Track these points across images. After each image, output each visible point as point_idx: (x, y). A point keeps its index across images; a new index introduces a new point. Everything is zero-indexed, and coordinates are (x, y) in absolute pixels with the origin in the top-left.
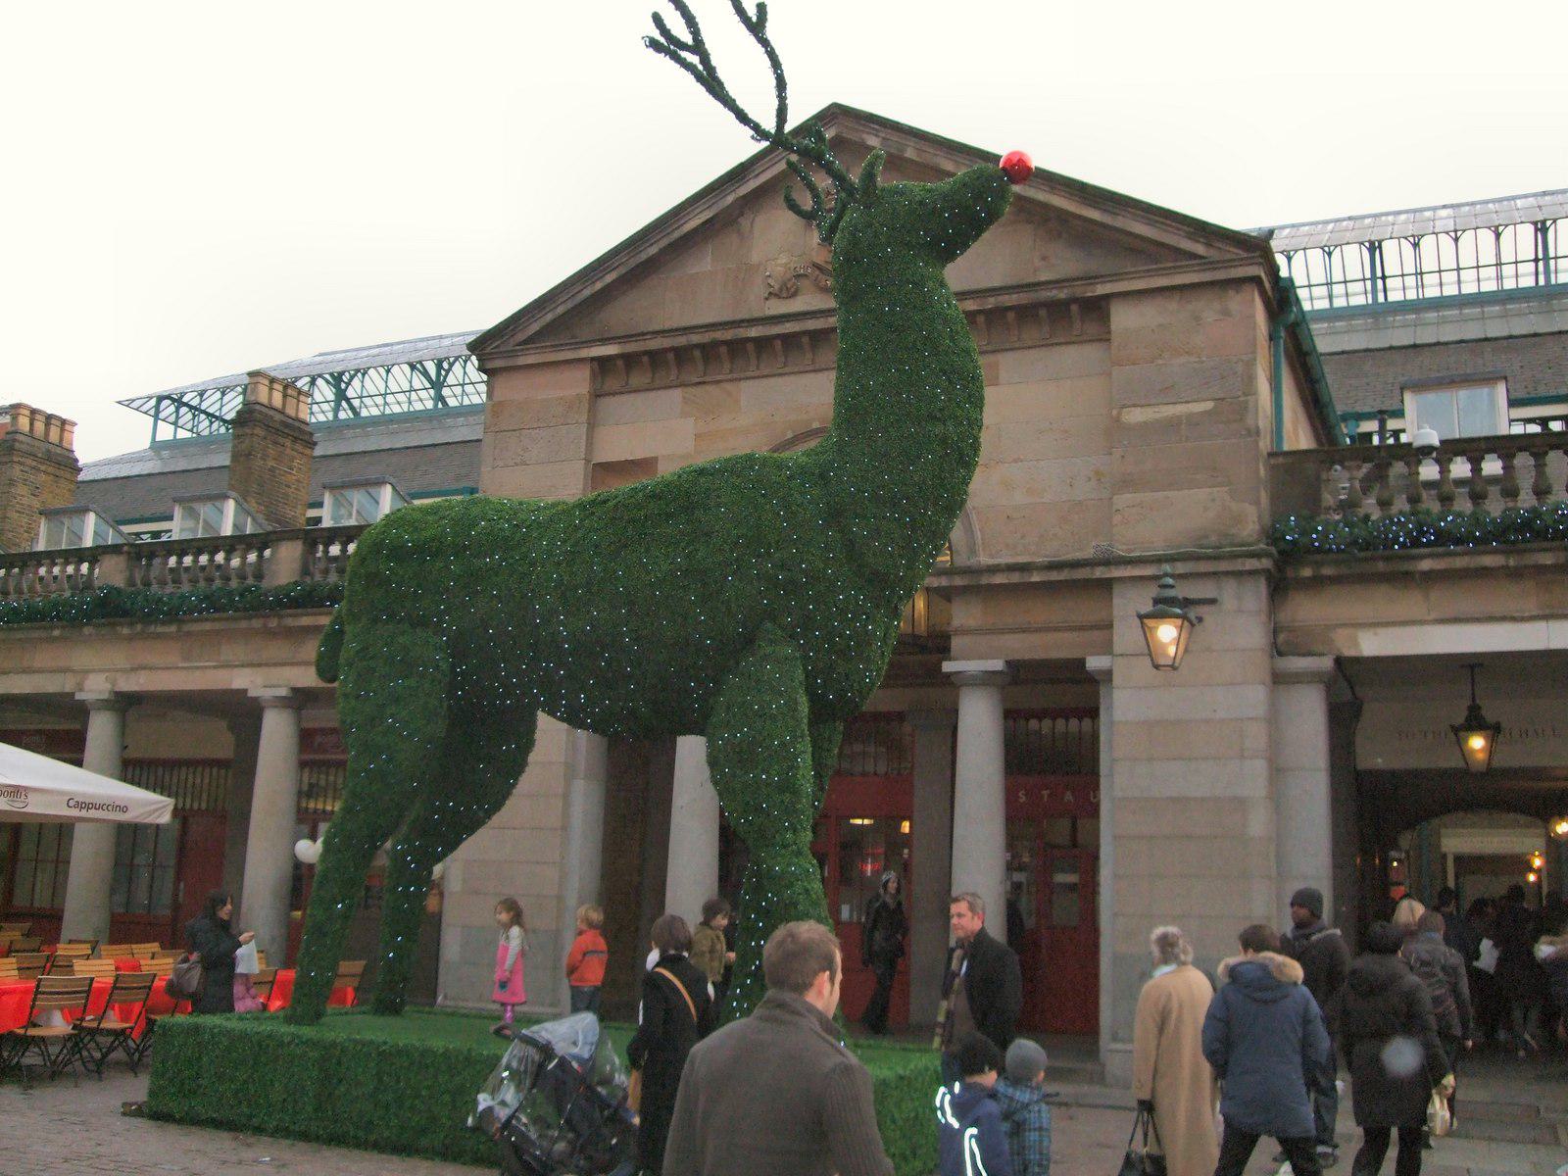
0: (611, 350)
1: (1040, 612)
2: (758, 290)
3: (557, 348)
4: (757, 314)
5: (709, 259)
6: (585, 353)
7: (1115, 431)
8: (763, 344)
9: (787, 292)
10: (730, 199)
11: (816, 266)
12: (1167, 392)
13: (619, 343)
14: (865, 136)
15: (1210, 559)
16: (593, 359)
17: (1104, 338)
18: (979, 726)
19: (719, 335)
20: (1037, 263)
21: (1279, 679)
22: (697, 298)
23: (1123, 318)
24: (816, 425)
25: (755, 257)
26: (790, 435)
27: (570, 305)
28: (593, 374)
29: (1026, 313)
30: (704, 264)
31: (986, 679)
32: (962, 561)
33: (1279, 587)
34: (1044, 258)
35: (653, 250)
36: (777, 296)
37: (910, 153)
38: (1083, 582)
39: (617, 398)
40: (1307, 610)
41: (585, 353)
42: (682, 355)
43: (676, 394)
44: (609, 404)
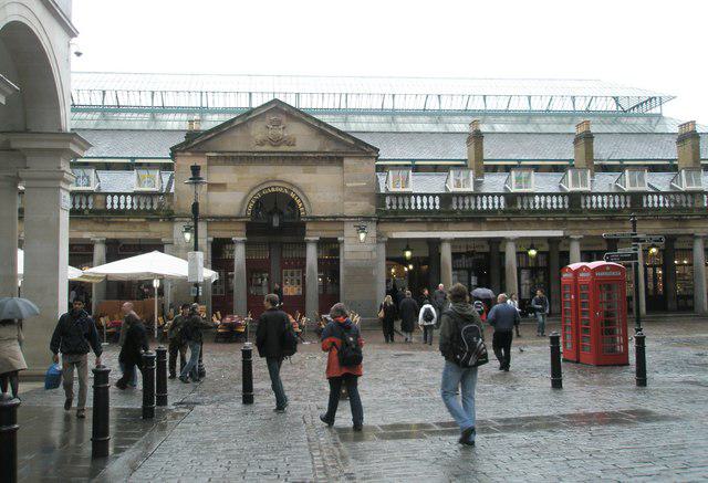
0: (214, 154)
1: (327, 227)
7: (344, 187)
9: (262, 144)
12: (357, 180)
15: (366, 218)
17: (341, 164)
18: (312, 254)
21: (378, 242)
22: (236, 143)
23: (347, 162)
25: (252, 133)
30: (238, 133)
31: (315, 242)
33: (378, 223)
38: (338, 220)
40: (384, 228)
44: (211, 167)
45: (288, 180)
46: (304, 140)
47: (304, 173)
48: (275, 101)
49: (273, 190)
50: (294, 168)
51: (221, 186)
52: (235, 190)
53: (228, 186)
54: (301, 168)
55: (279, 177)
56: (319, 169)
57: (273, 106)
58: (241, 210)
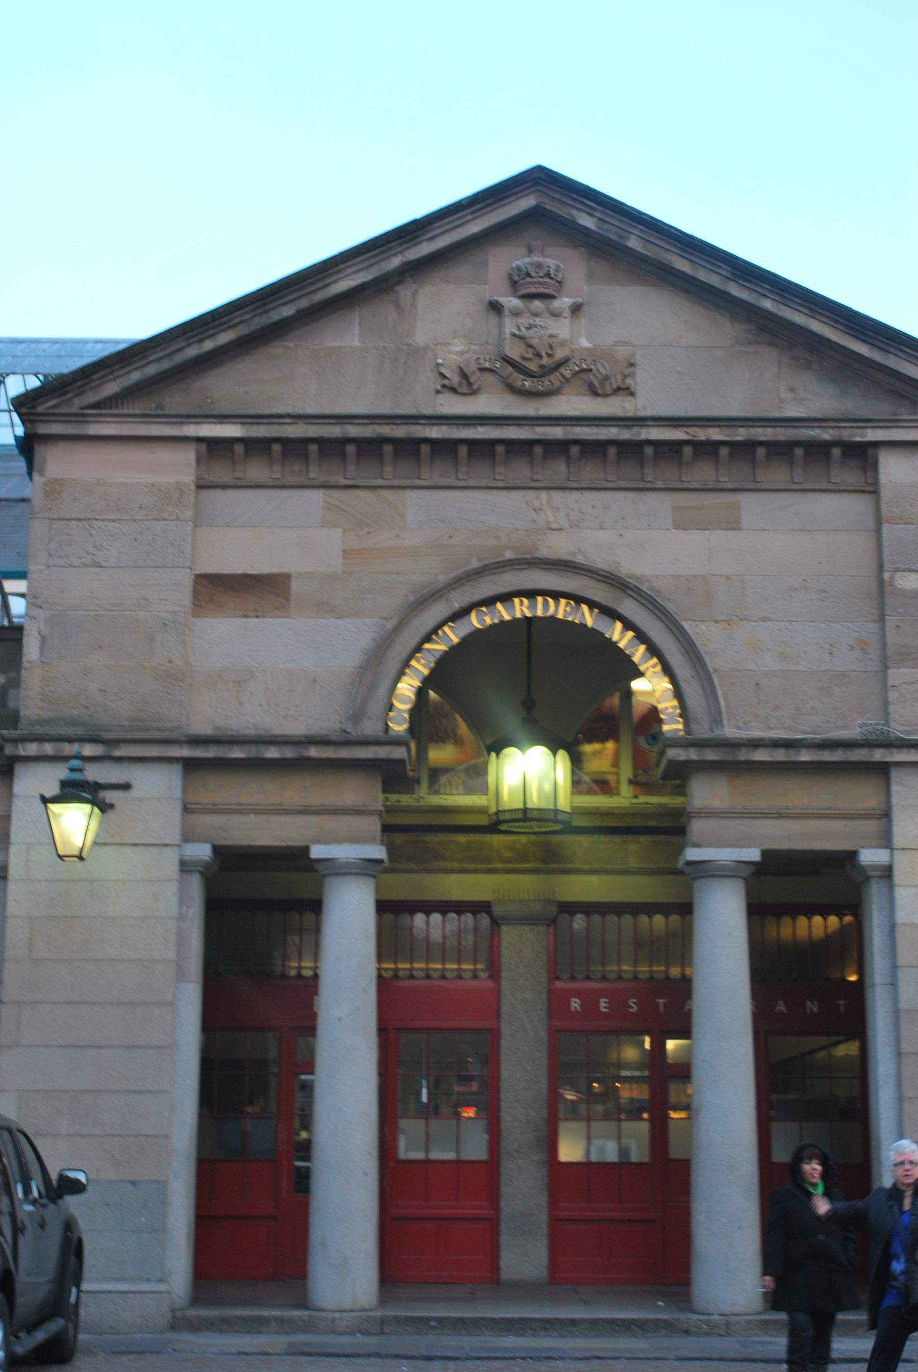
2: (427, 380)
3: (146, 417)
4: (428, 411)
5: (356, 330)
6: (191, 430)
8: (444, 449)
10: (396, 262)
11: (507, 360)
13: (243, 424)
14: (574, 212)
16: (199, 440)
19: (386, 431)
20: (784, 394)
24: (509, 555)
26: (475, 564)
27: (166, 365)
28: (199, 461)
29: (780, 451)
32: (702, 731)
34: (791, 390)
35: (288, 311)
36: (453, 390)
37: (633, 243)
39: (229, 493)
41: (191, 430)
42: (332, 449)
43: (317, 497)
45: (601, 561)
46: (676, 371)
47: (681, 525)
48: (540, 179)
49: (521, 608)
50: (619, 502)
51: (255, 591)
52: (324, 608)
53: (295, 586)
54: (659, 505)
55: (556, 546)
56: (750, 504)
57: (526, 203)
58: (357, 717)
